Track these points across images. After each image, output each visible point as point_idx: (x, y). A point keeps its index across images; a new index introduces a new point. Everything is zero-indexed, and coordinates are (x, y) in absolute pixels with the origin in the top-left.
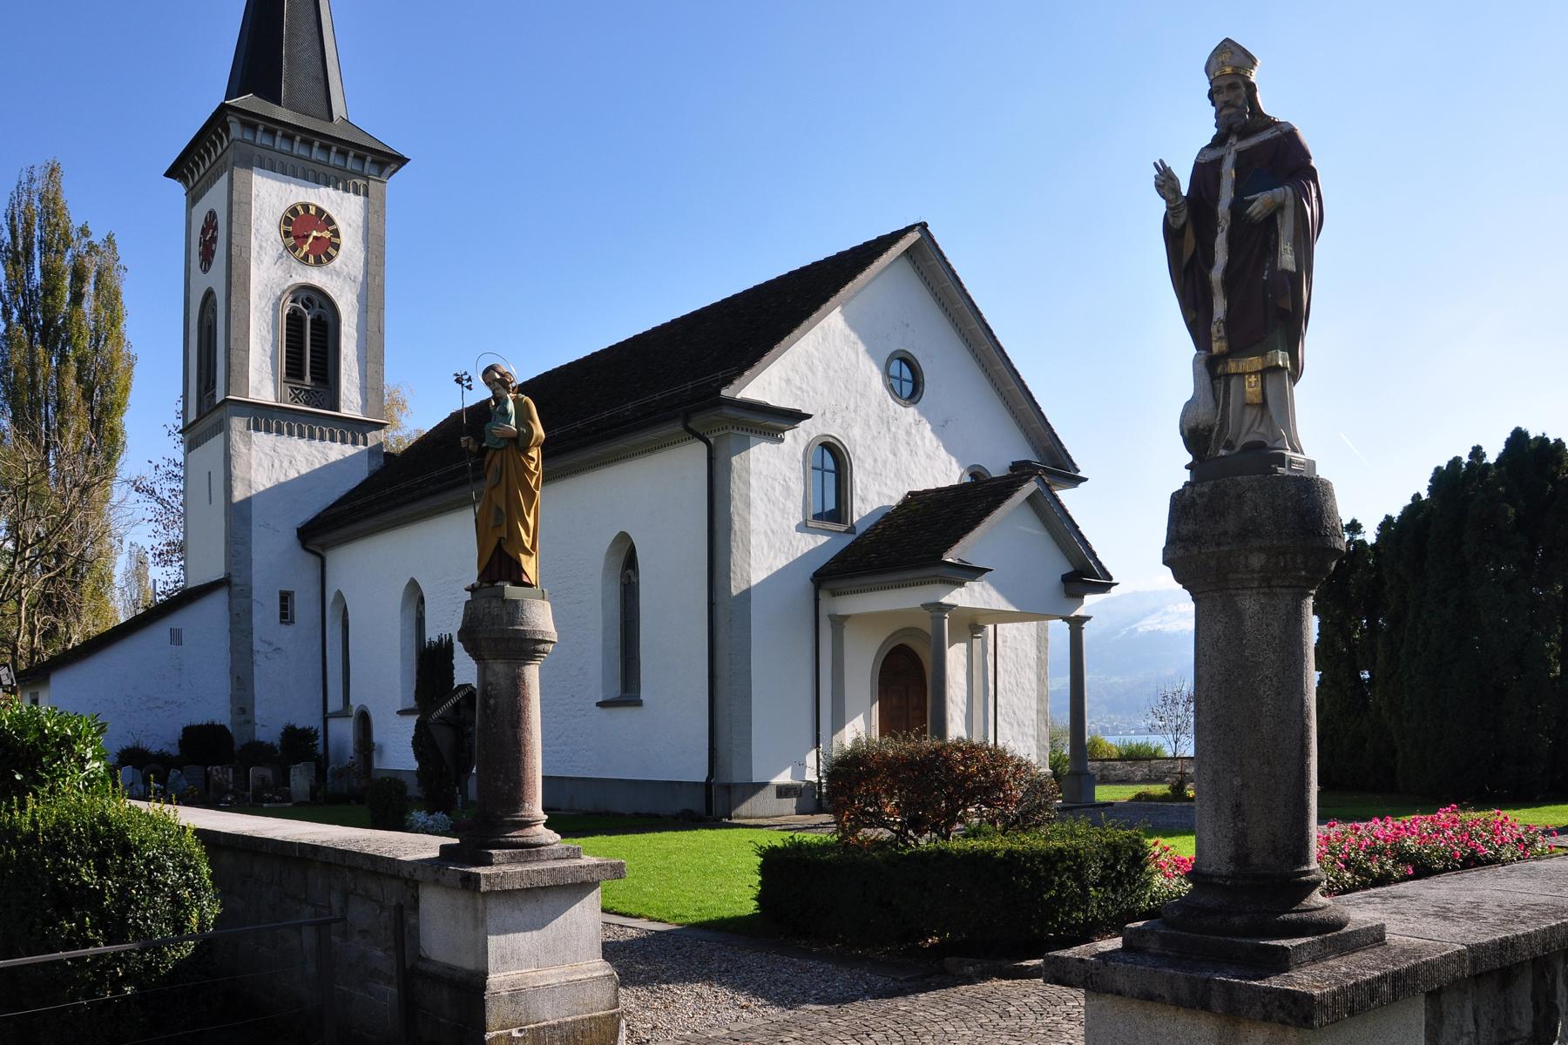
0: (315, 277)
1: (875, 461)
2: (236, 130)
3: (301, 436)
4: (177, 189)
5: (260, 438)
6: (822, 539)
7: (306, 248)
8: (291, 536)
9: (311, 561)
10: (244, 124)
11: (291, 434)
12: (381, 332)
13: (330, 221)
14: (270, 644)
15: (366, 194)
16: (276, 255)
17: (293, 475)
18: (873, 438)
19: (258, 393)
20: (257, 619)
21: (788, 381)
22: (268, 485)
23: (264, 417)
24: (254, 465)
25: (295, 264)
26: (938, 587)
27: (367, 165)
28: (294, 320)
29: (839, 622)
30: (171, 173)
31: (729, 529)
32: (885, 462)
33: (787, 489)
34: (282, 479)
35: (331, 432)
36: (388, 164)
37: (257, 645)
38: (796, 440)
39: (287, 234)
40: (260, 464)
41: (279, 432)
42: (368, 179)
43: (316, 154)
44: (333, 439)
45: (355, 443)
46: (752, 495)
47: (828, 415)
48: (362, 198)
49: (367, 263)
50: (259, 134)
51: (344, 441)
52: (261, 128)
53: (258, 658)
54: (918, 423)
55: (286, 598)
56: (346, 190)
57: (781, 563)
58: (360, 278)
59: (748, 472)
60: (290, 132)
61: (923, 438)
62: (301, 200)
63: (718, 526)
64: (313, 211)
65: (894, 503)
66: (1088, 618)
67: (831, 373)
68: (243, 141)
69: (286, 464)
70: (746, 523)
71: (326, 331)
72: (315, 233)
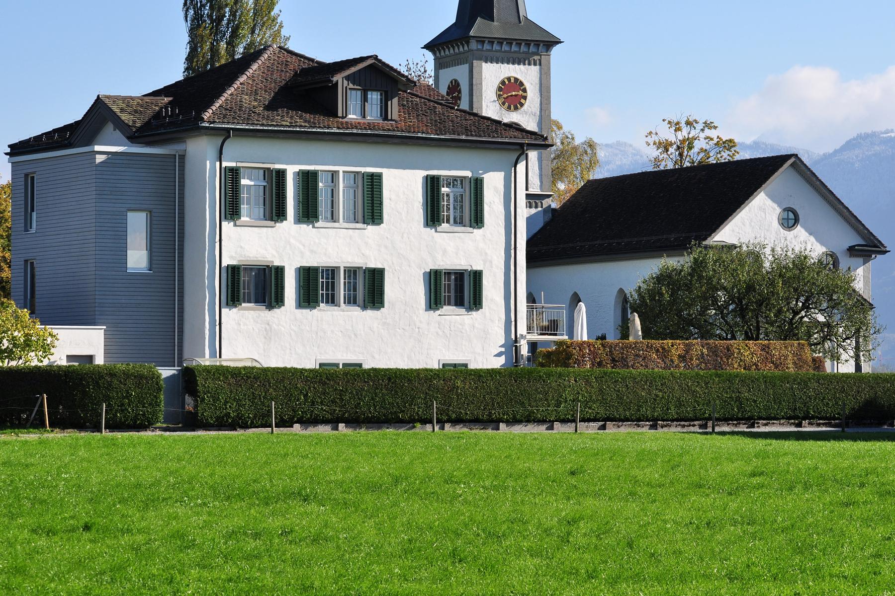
13: (522, 84)
15: (540, 65)
21: (733, 231)
25: (504, 111)
45: (536, 207)
48: (538, 67)
56: (529, 64)
62: (507, 76)
64: (512, 81)
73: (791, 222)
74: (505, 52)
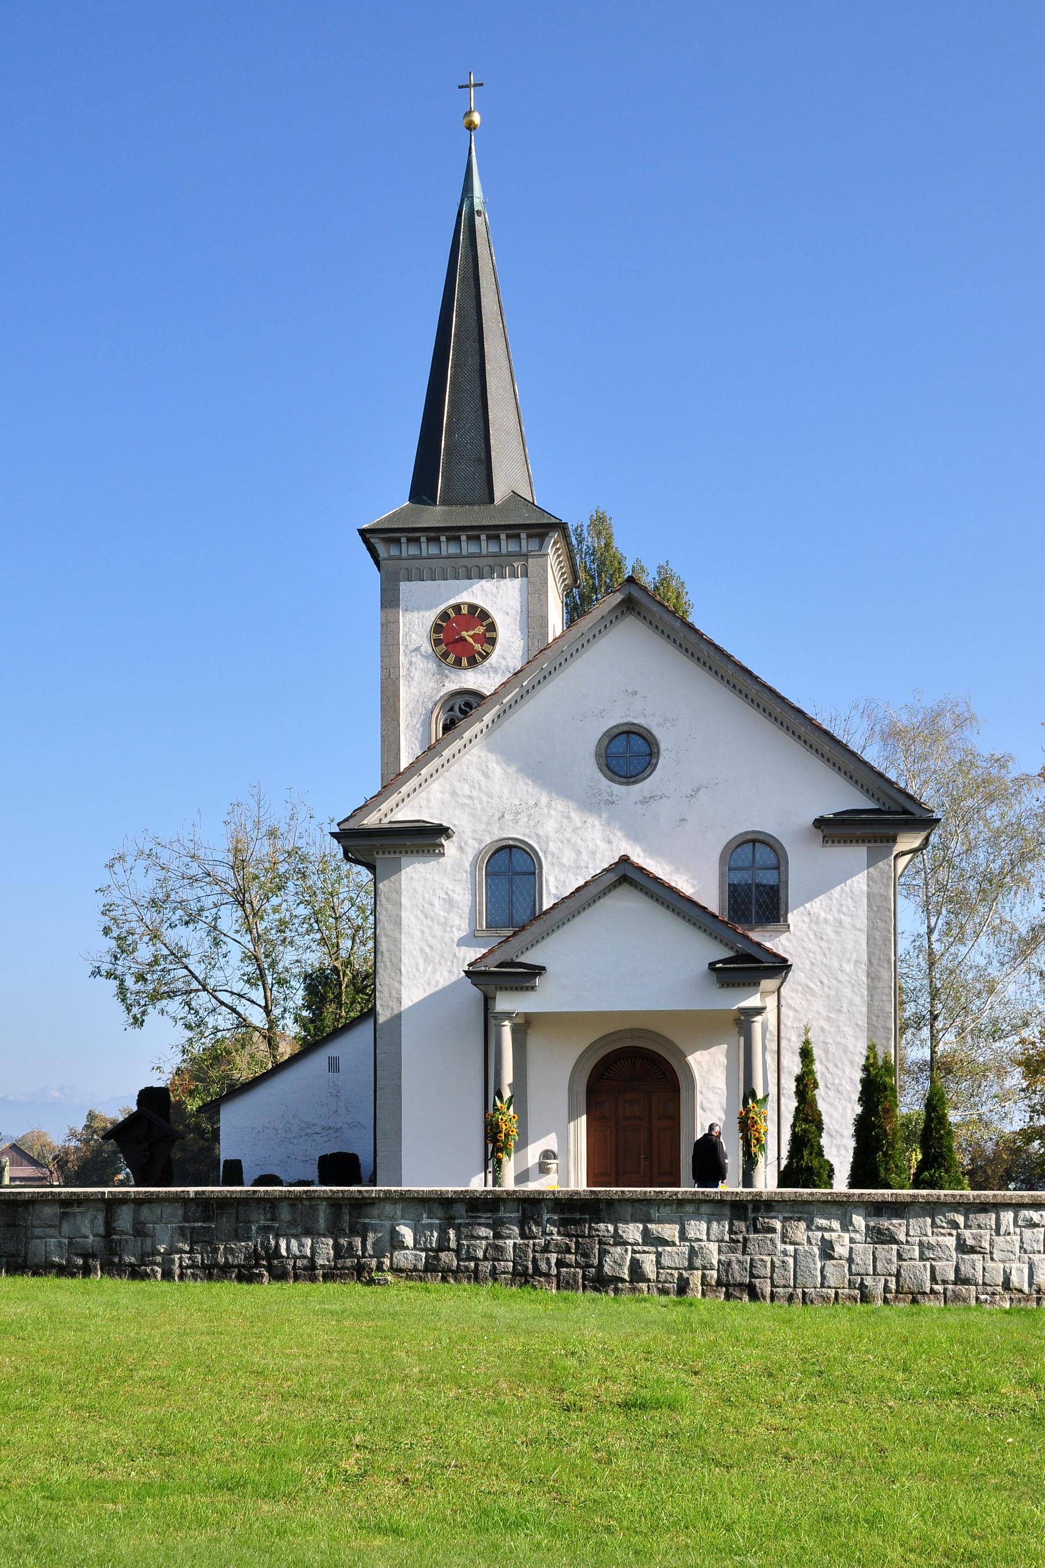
1: (579, 852)
10: (389, 541)
13: (485, 615)
18: (575, 830)
21: (454, 793)
32: (593, 853)
33: (450, 904)
39: (437, 642)
47: (506, 817)
48: (517, 582)
56: (502, 576)
59: (399, 892)
64: (465, 611)
68: (391, 558)
70: (397, 942)
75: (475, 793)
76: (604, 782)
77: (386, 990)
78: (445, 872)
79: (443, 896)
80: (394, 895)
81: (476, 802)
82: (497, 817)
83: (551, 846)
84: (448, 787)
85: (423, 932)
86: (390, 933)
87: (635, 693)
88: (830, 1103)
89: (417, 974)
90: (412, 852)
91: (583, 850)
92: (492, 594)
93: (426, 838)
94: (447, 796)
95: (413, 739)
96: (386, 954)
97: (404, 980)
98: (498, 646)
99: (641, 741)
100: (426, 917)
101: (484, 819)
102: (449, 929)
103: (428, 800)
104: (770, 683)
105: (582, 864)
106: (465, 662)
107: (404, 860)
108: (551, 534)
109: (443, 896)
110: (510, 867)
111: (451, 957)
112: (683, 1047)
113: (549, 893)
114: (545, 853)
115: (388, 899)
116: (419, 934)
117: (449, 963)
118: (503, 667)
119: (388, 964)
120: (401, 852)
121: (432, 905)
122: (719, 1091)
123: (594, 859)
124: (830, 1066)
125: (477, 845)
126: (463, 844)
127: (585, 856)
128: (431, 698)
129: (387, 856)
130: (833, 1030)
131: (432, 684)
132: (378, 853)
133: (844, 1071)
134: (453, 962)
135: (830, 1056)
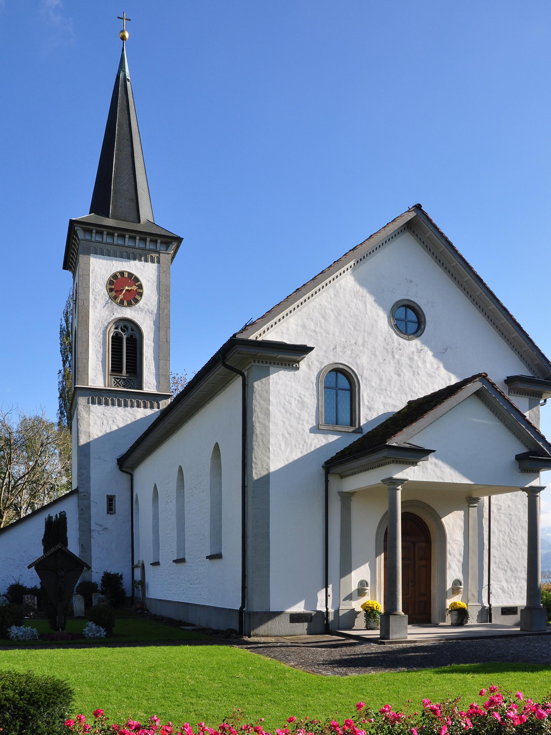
0: (128, 313)
1: (381, 380)
2: (81, 234)
3: (119, 405)
4: (69, 273)
5: (96, 409)
6: (333, 438)
7: (121, 296)
8: (114, 463)
9: (126, 477)
11: (113, 404)
12: (168, 341)
13: (137, 280)
14: (101, 526)
15: (159, 262)
16: (104, 302)
17: (115, 428)
18: (379, 364)
19: (94, 381)
20: (93, 511)
21: (304, 327)
22: (100, 435)
23: (98, 396)
24: (92, 424)
25: (115, 306)
26: (391, 466)
27: (158, 245)
28: (116, 340)
29: (347, 498)
30: (65, 268)
31: (252, 432)
32: (390, 381)
33: (302, 404)
34: (108, 431)
35: (138, 402)
36: (171, 243)
37: (93, 527)
38: (310, 368)
39: (111, 290)
40: (95, 423)
41: (107, 404)
42: (159, 253)
43: (128, 242)
44: (138, 406)
45: (152, 407)
46: (271, 408)
47: (338, 349)
48: (156, 265)
49: (159, 302)
50: (94, 235)
51: (145, 407)
52: (94, 231)
53: (94, 534)
54: (420, 351)
55: (111, 500)
56: (146, 261)
57: (296, 455)
58: (155, 311)
59: (268, 392)
60: (111, 231)
61: (424, 362)
62: (119, 270)
63: (248, 432)
64: (126, 275)
65: (397, 410)
66: (543, 488)
67: (342, 319)
69: (110, 422)
70: (266, 428)
71: (136, 344)
72: (127, 288)
73: (413, 327)
74: (118, 245)
75: (318, 329)
76: (395, 335)
77: (259, 462)
78: (299, 381)
79: (297, 398)
80: (265, 394)
81: (319, 335)
82: (332, 347)
83: (365, 371)
84: (300, 322)
85: (284, 422)
86: (262, 421)
87: (411, 281)
88: (512, 551)
89: (280, 453)
90: (278, 364)
91: (383, 378)
92: (141, 269)
93: (290, 355)
94: (300, 329)
95: (96, 341)
96: (259, 436)
97: (271, 456)
98: (143, 297)
99: (413, 313)
100: (286, 412)
101: (324, 348)
102: (301, 422)
103: (288, 329)
104: (491, 289)
105: (383, 387)
106: (125, 303)
107: (271, 369)
108: (173, 243)
109: (297, 398)
110: (341, 384)
111: (302, 442)
112: (439, 513)
113: (364, 405)
114: (361, 376)
115: (261, 396)
116: (281, 423)
117: (301, 446)
118: (146, 309)
119: (261, 443)
120: (270, 363)
121: (290, 404)
122: (458, 543)
123: (390, 385)
124: (512, 529)
125: (319, 365)
126: (310, 363)
127: (385, 382)
128: (106, 320)
129: (261, 364)
130: (514, 507)
131: (107, 313)
132: (255, 361)
133: (518, 532)
134: (303, 446)
135: (512, 522)
